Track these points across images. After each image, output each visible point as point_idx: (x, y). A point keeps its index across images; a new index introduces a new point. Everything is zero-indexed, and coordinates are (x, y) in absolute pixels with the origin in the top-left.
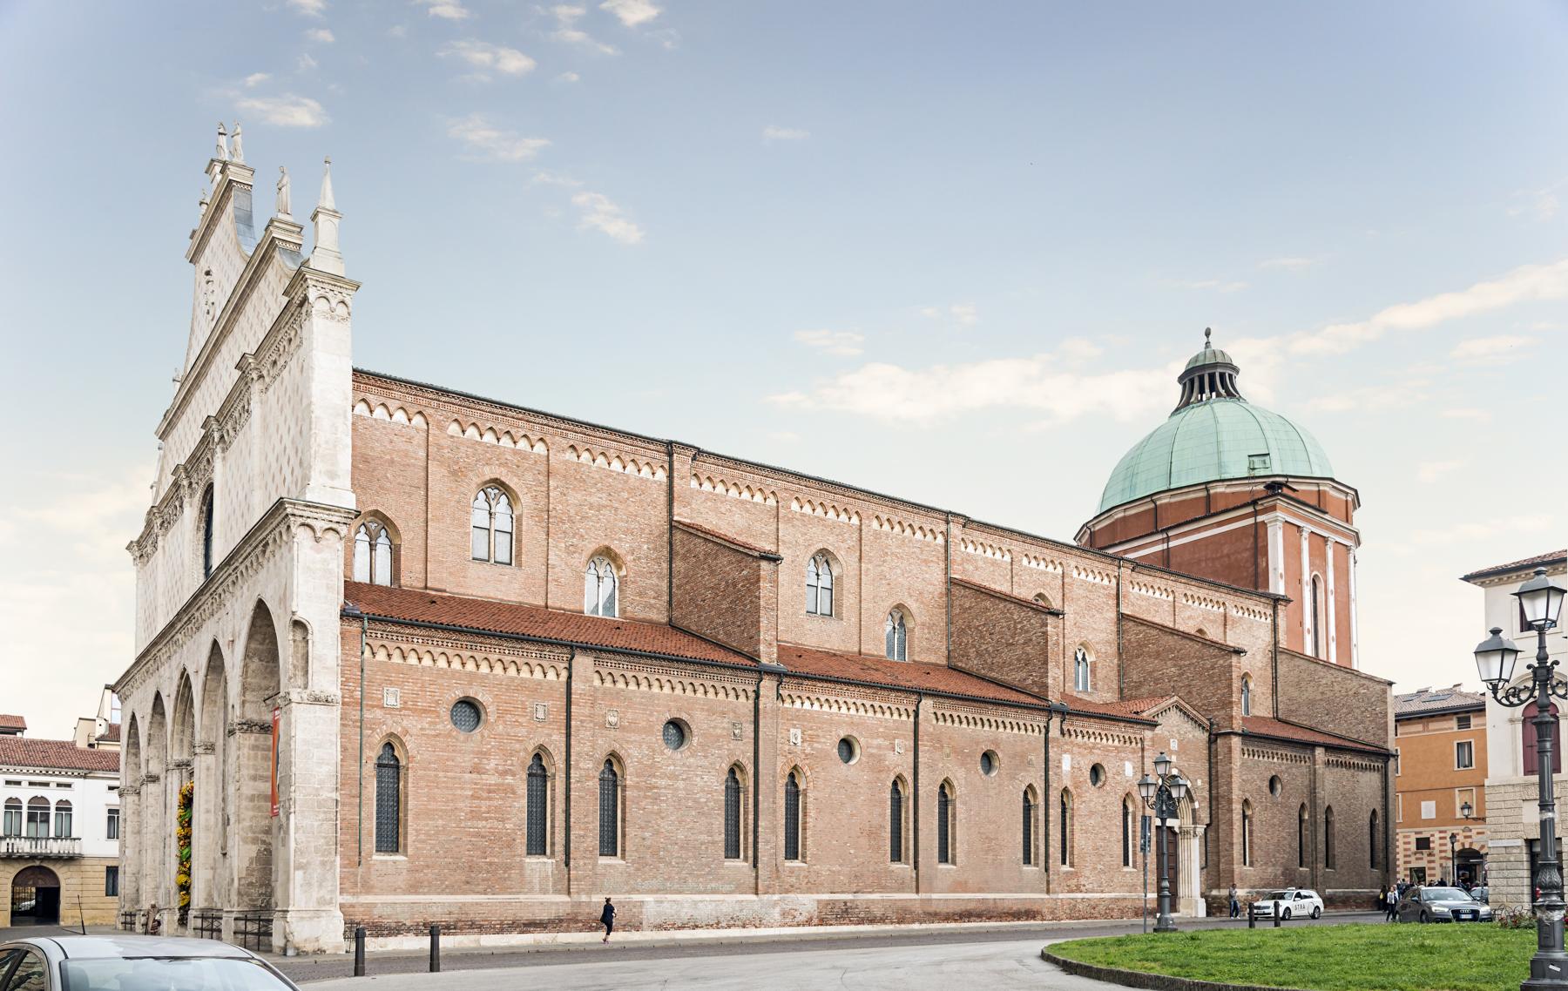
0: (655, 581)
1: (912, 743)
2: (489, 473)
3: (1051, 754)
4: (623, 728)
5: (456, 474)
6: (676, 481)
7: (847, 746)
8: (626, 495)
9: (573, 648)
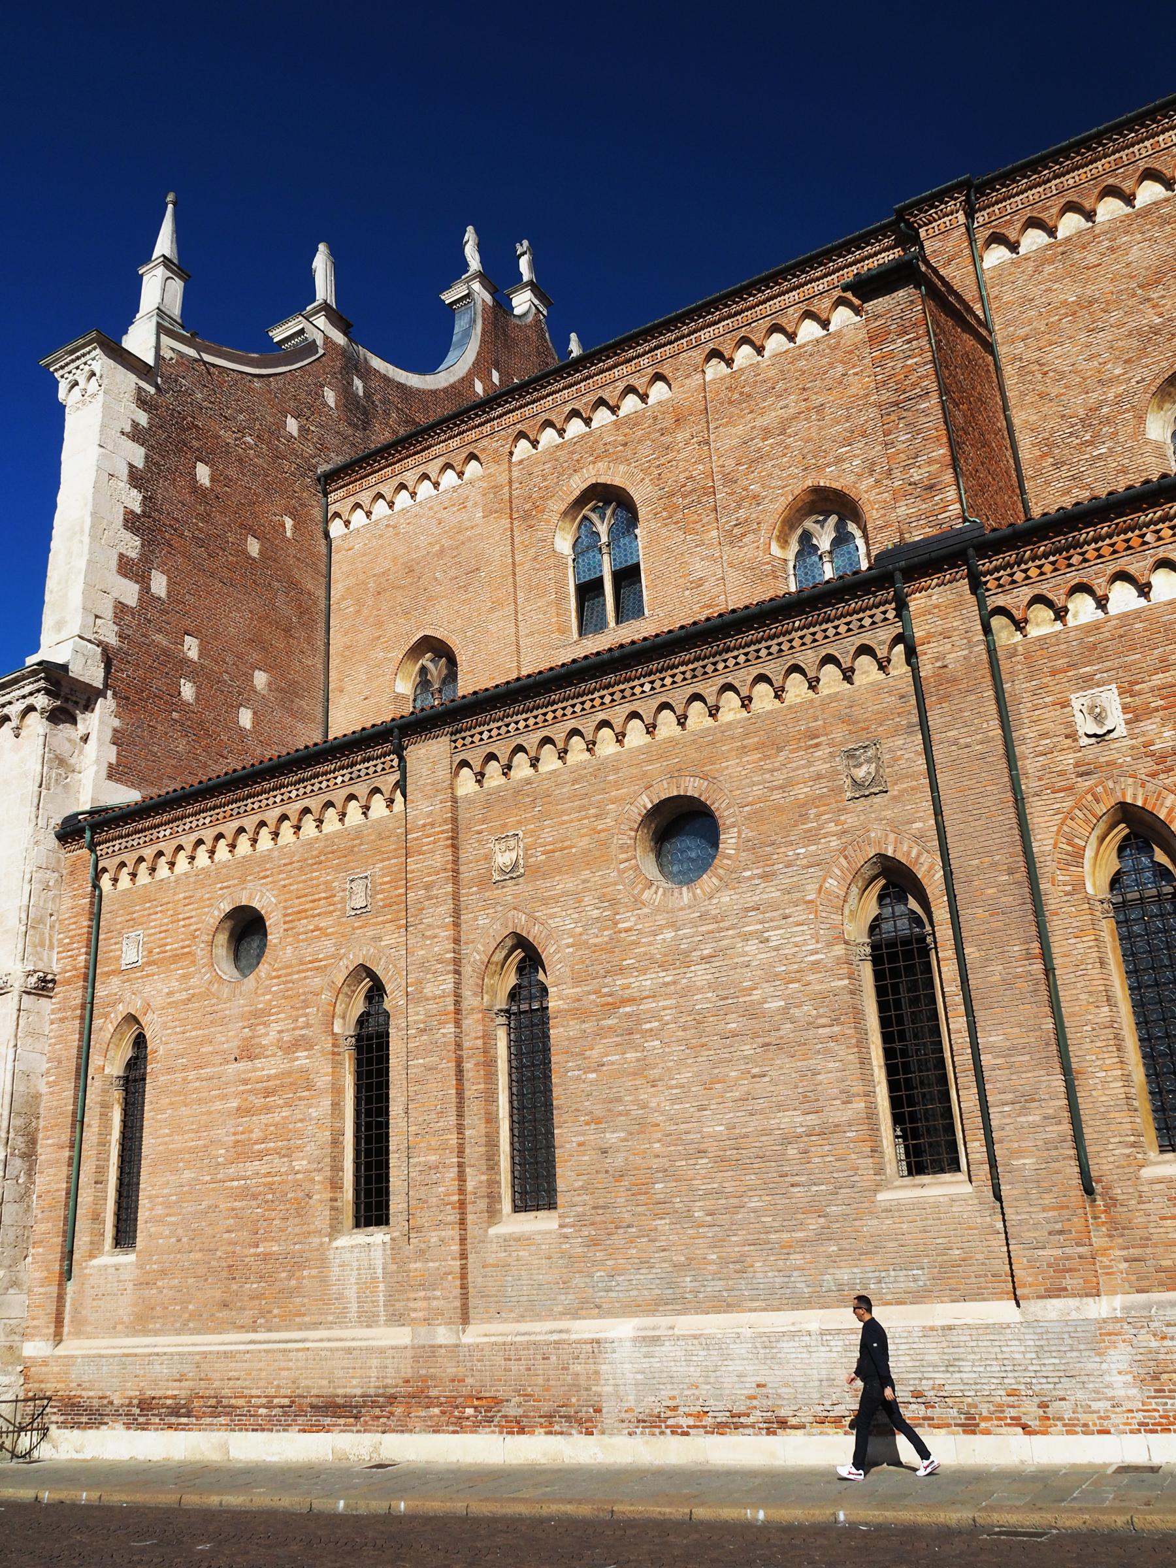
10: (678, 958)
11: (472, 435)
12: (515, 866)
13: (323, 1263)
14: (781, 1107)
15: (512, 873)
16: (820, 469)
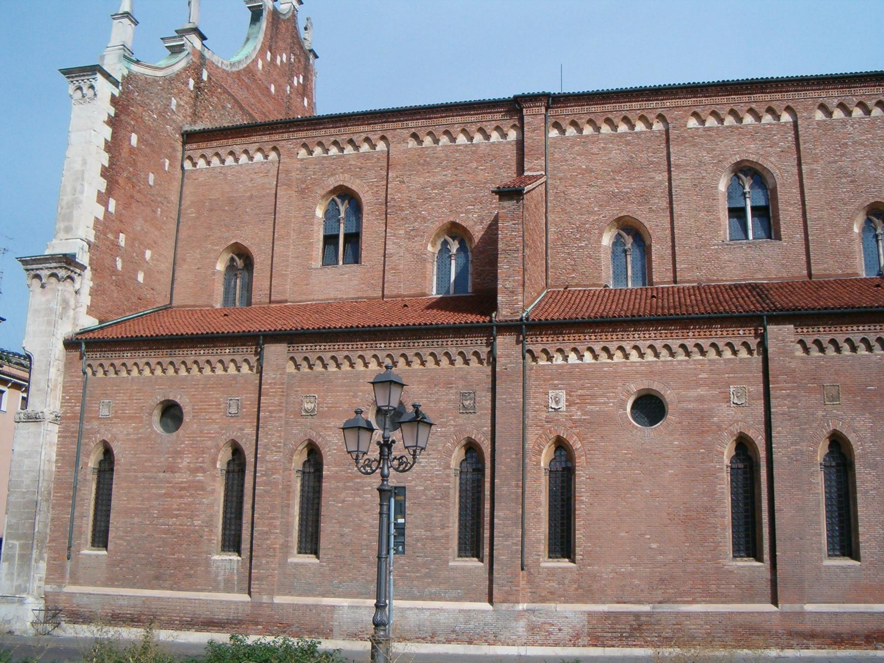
1: (761, 388)
7: (650, 407)
11: (277, 137)
12: (314, 410)
14: (417, 527)
15: (311, 413)
16: (458, 213)
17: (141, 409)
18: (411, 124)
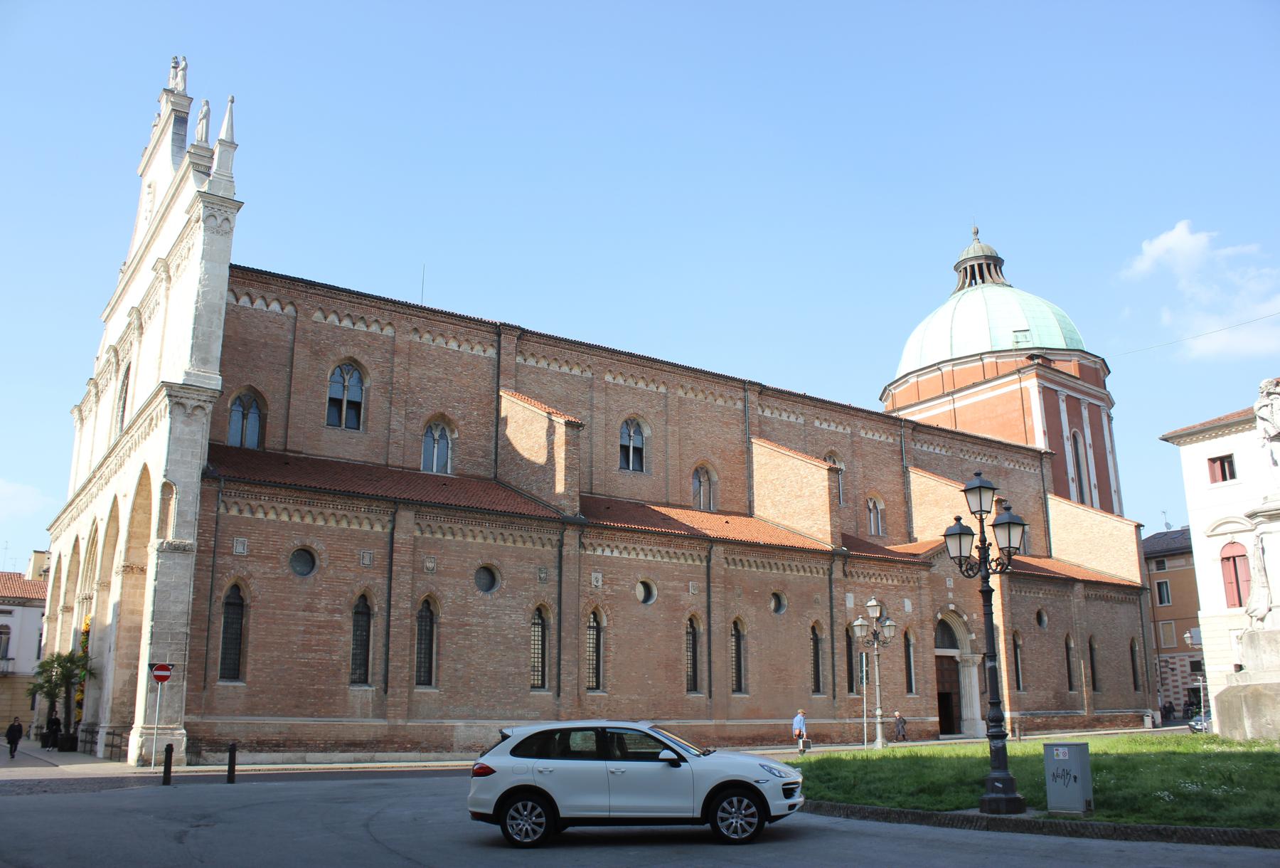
0: (483, 442)
2: (345, 352)
3: (835, 593)
4: (439, 573)
5: (317, 354)
6: (503, 357)
8: (460, 369)
9: (396, 504)
10: (484, 615)
13: (346, 694)
17: (278, 550)
18: (415, 319)
